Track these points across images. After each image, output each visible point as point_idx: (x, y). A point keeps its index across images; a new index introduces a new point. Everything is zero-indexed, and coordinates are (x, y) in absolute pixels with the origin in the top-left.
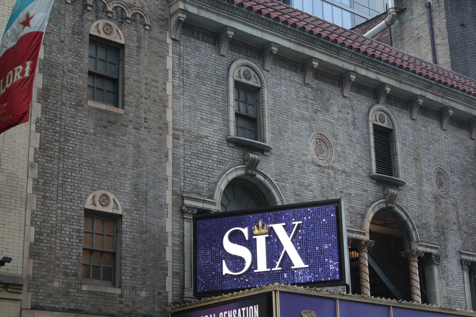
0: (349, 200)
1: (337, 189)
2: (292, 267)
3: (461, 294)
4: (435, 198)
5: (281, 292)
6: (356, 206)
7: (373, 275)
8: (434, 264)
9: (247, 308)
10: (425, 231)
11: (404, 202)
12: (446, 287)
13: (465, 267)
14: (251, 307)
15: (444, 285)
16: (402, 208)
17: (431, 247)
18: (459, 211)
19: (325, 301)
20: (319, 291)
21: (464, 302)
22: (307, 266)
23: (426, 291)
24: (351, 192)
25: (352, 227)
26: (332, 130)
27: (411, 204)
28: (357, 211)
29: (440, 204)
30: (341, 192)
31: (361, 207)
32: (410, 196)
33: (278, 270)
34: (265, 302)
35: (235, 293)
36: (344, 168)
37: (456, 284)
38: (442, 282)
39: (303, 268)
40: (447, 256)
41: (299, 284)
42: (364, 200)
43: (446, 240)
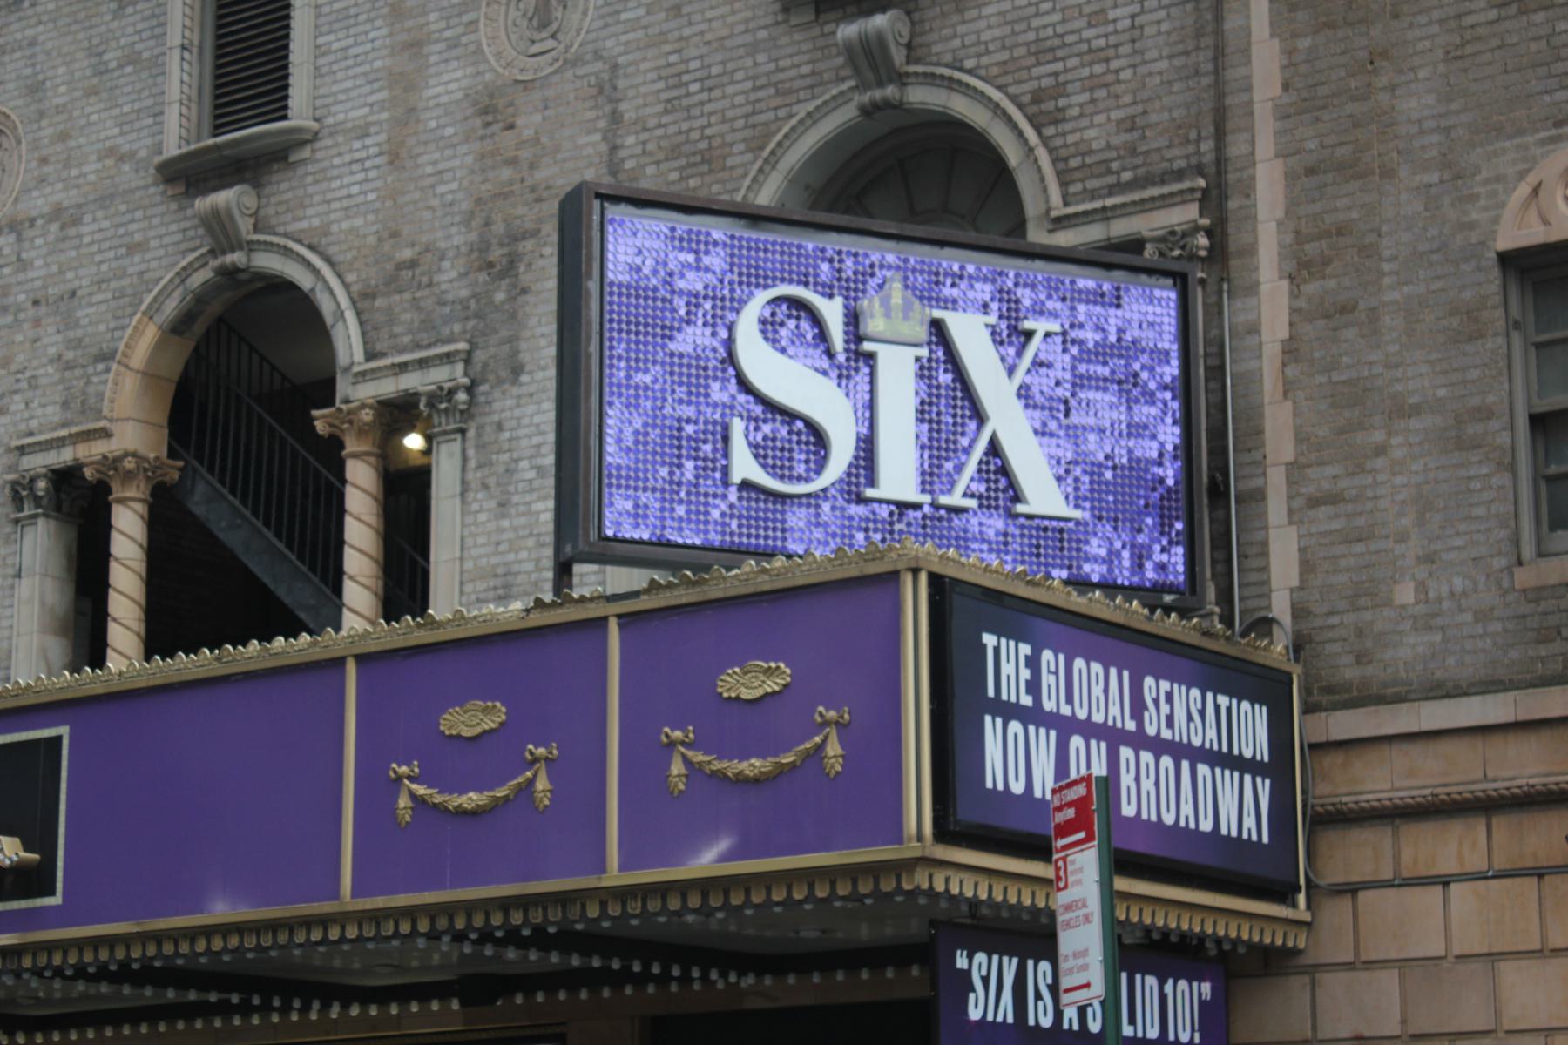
0: (69, 322)
1: (22, 297)
4: (485, 111)
6: (90, 330)
10: (407, 296)
11: (310, 212)
16: (285, 247)
17: (423, 364)
18: (623, 106)
24: (77, 283)
25: (64, 425)
26: (29, 71)
27: (345, 203)
28: (94, 351)
29: (511, 127)
30: (36, 303)
31: (112, 325)
32: (346, 170)
36: (57, 197)
38: (475, 507)
40: (517, 370)
42: (129, 291)
43: (524, 291)
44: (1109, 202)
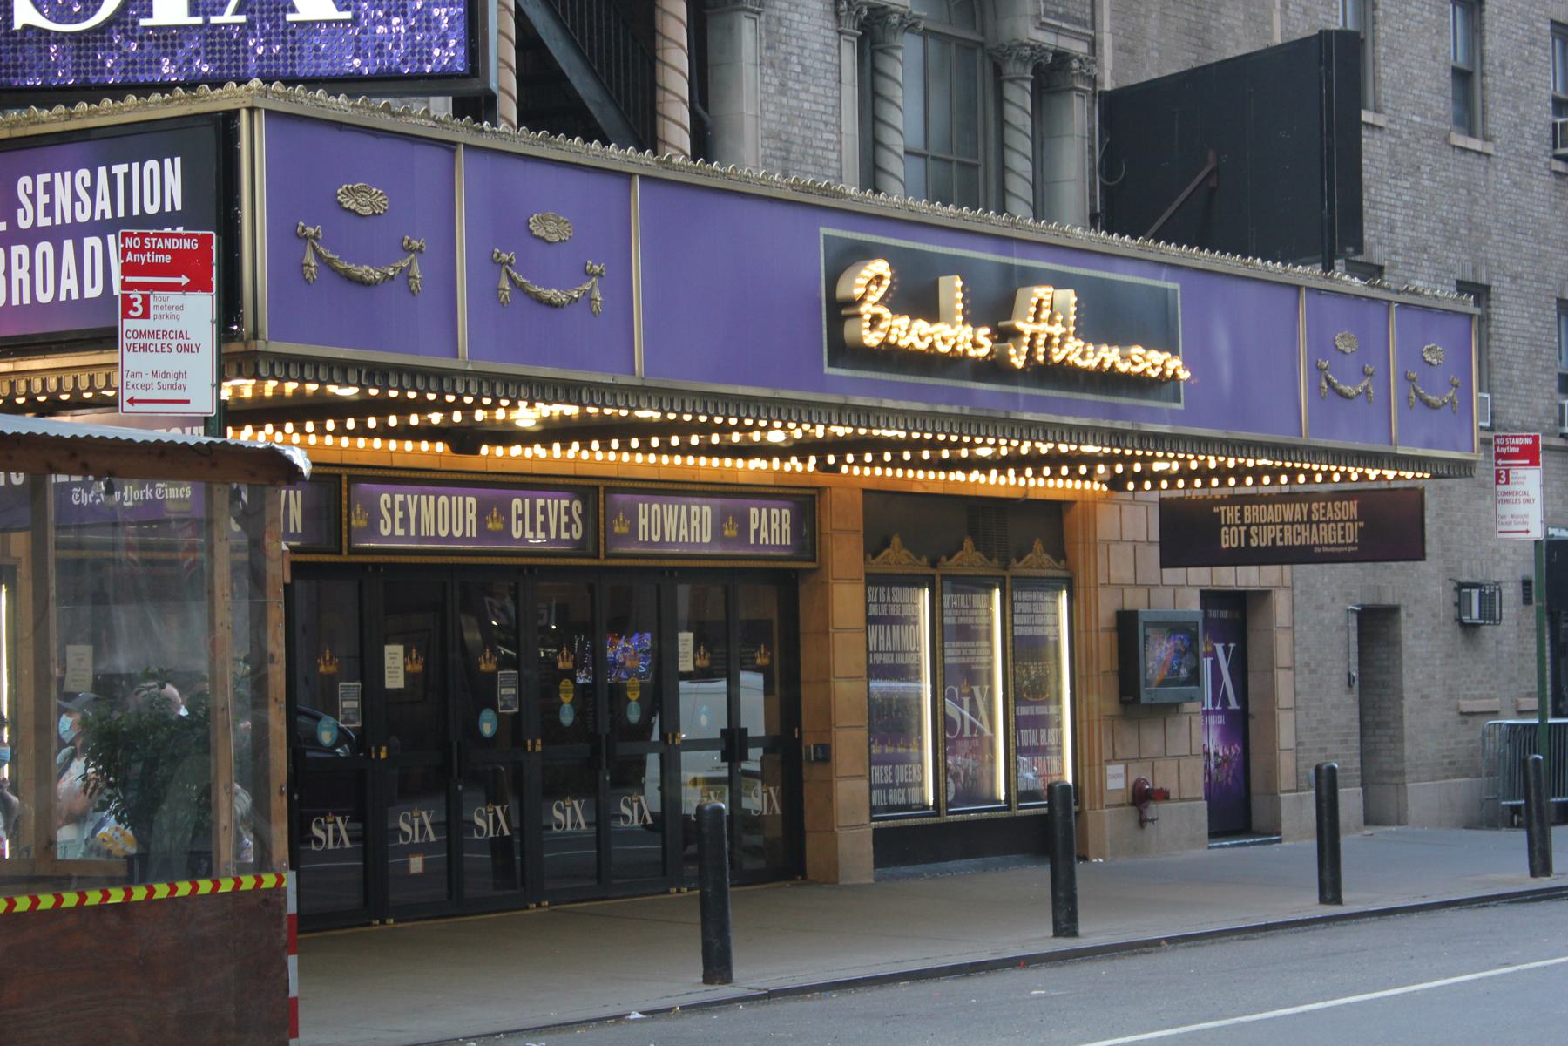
2: (290, 17)
3: (826, 123)
5: (269, 112)
7: (528, 42)
8: (745, 9)
9: (136, 166)
12: (777, 99)
13: (851, 27)
14: (152, 164)
15: (772, 90)
19: (421, 151)
20: (400, 115)
21: (834, 156)
22: (347, 15)
23: (706, 108)
33: (235, 25)
34: (212, 149)
35: (83, 106)
37: (812, 89)
38: (767, 79)
39: (328, 23)
41: (312, 82)
44: (1064, 25)
